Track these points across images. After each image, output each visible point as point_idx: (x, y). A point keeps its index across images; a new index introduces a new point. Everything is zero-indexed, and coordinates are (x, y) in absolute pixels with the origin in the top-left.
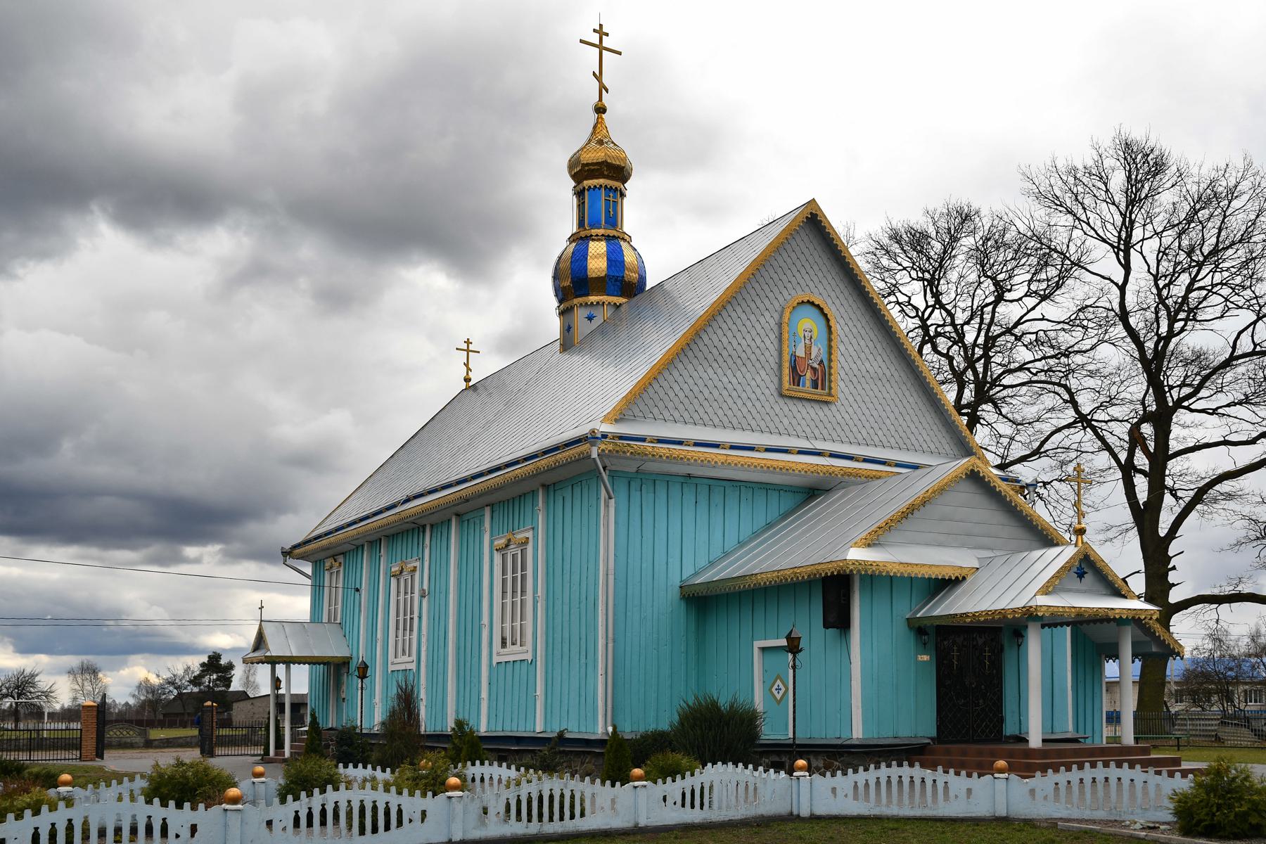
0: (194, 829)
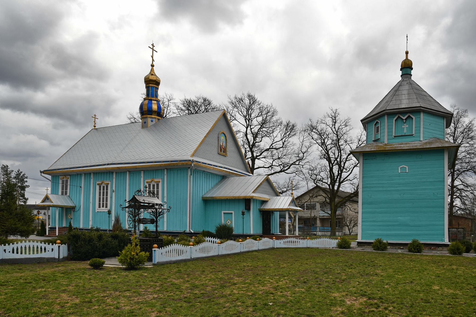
0: (52, 250)
